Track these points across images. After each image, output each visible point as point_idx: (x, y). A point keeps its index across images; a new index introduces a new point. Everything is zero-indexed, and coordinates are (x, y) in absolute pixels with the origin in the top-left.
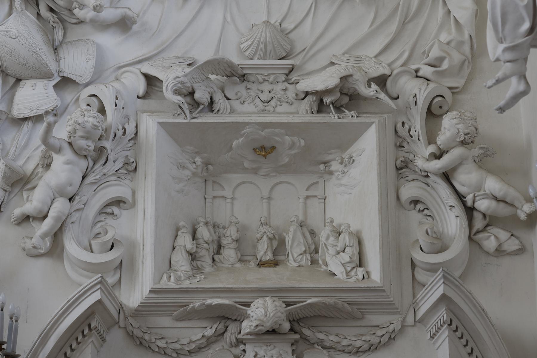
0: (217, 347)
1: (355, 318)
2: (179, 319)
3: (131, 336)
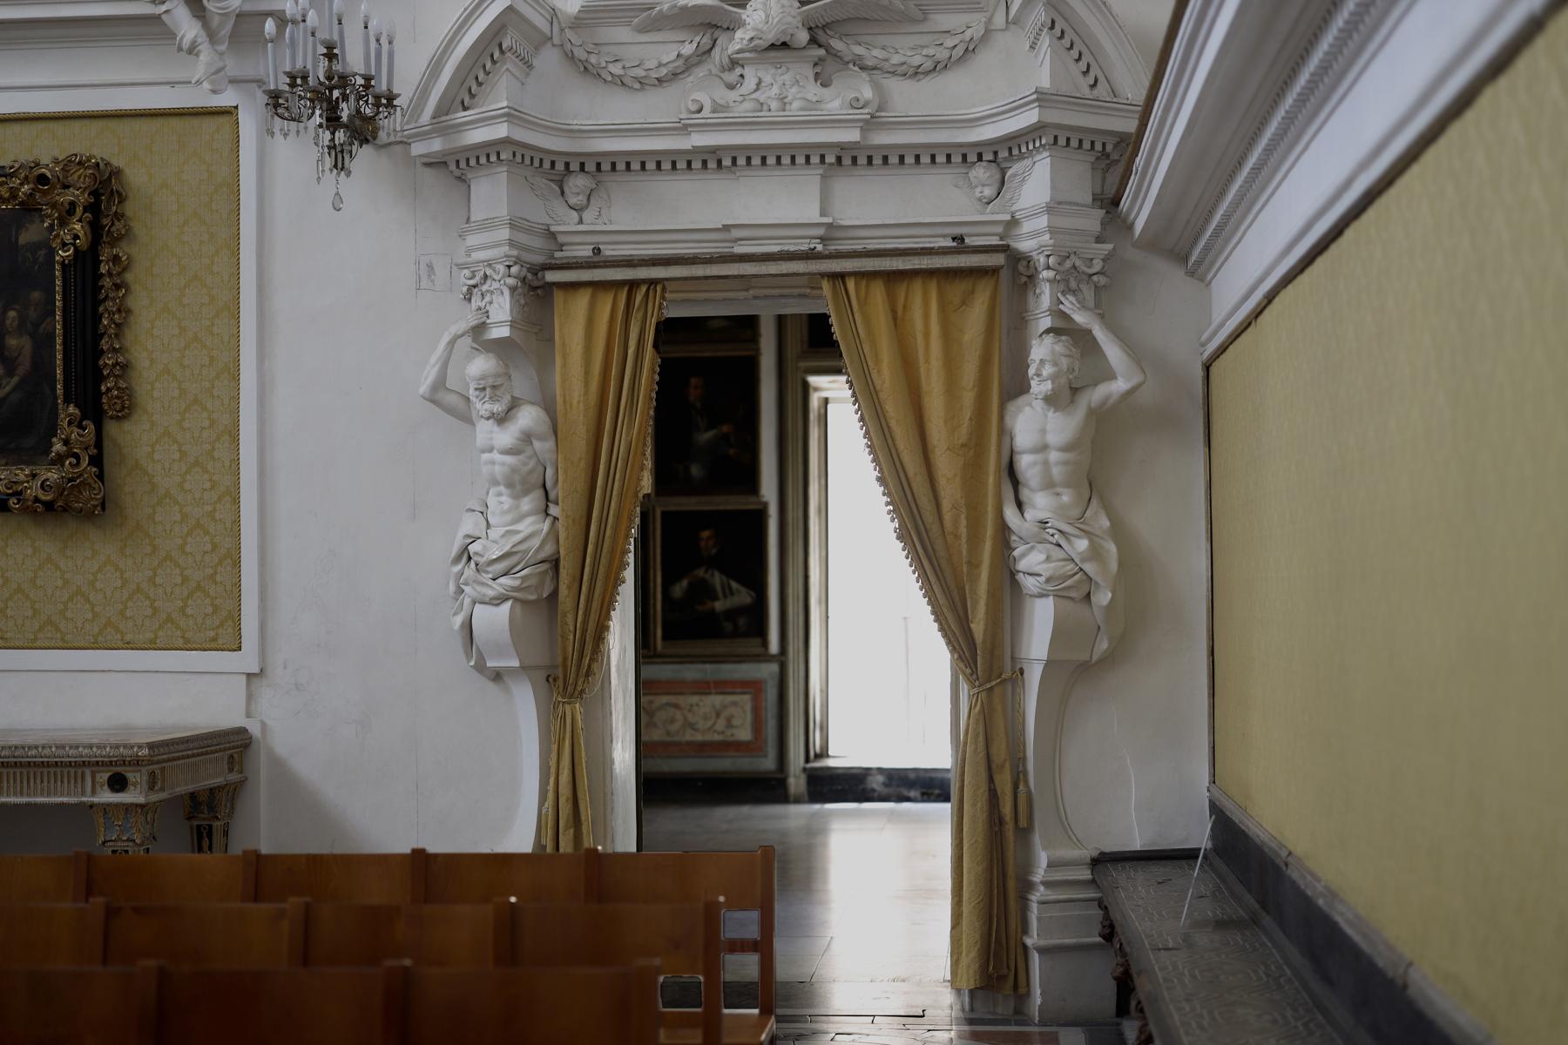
0: (700, 72)
1: (914, 21)
2: (642, 30)
3: (570, 58)
